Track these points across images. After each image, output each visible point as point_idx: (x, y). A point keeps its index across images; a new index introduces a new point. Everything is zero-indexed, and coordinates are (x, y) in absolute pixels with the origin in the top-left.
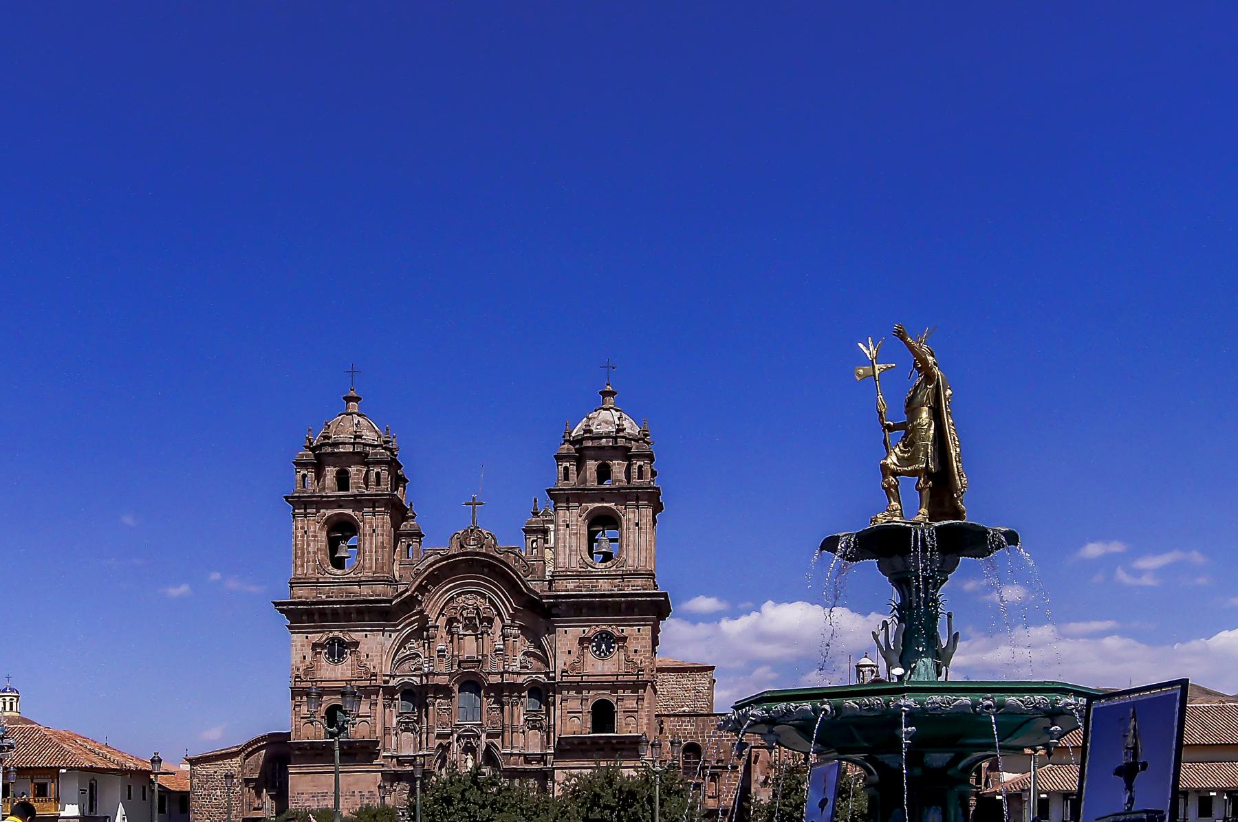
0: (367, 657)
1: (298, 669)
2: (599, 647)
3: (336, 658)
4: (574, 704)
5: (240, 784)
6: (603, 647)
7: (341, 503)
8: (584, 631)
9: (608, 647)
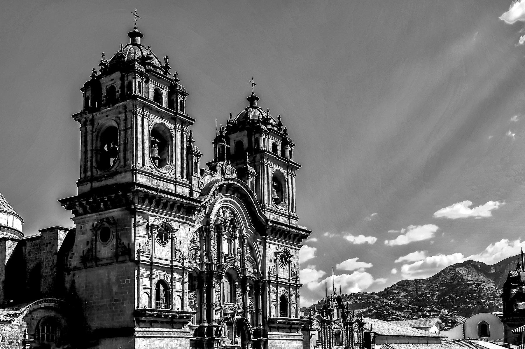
0: (180, 244)
1: (140, 245)
2: (282, 259)
3: (163, 241)
4: (273, 296)
5: (19, 345)
6: (284, 260)
7: (163, 115)
8: (276, 248)
9: (286, 261)
